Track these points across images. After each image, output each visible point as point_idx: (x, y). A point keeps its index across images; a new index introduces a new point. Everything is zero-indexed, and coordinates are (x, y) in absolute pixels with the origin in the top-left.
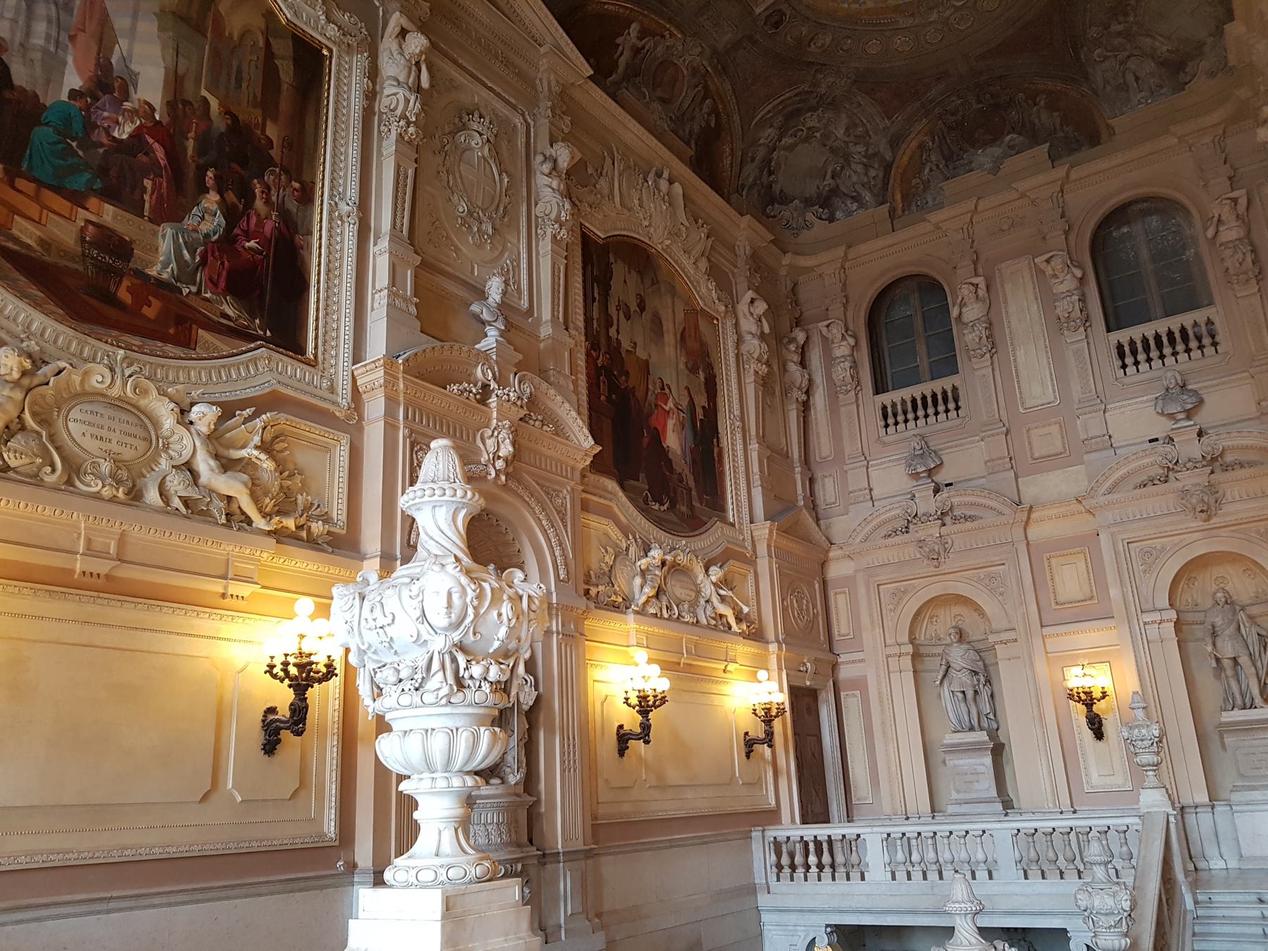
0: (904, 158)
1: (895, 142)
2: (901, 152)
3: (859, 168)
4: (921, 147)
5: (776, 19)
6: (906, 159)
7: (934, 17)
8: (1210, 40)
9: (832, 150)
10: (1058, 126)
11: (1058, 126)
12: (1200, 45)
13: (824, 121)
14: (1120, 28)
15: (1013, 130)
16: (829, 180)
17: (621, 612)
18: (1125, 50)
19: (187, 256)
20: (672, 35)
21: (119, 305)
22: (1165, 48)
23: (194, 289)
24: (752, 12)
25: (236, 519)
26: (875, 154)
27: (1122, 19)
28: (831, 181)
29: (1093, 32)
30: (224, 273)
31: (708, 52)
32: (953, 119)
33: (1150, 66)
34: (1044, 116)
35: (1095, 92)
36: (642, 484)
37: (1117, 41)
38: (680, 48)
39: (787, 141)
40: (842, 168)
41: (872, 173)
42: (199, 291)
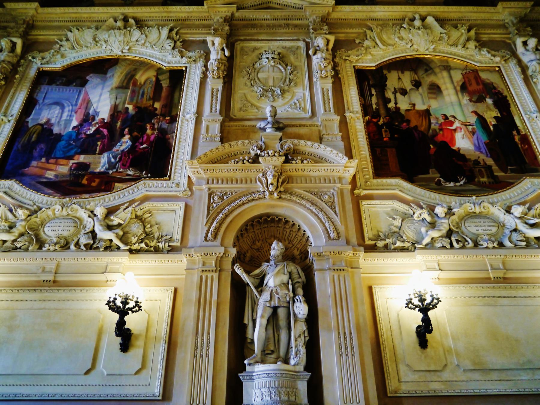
17: (411, 251)
19: (113, 160)
21: (84, 185)
23: (114, 170)
25: (109, 248)
30: (129, 160)
36: (434, 174)
42: (117, 170)
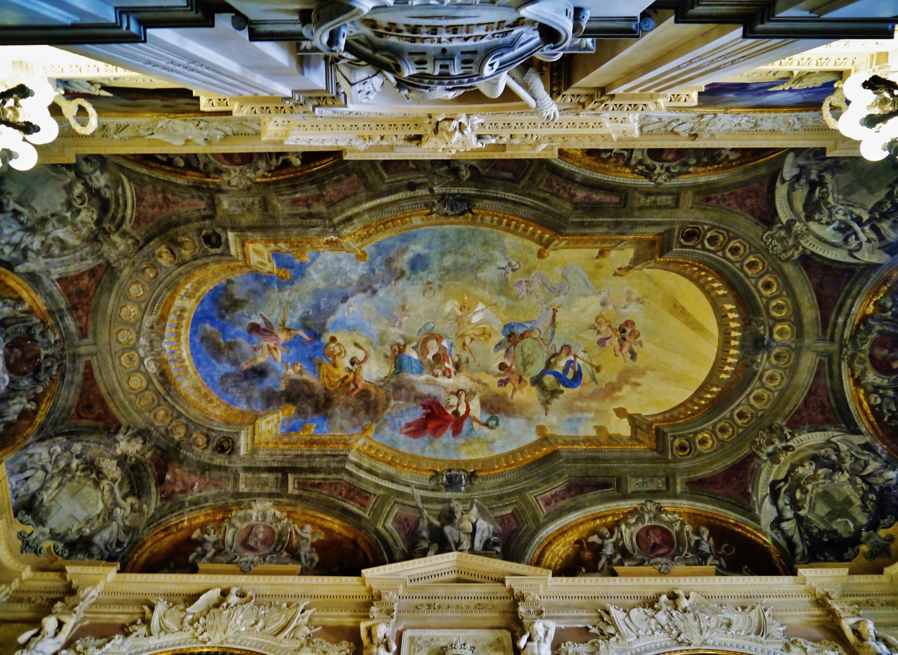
0: (12, 281)
1: (33, 278)
2: (20, 281)
3: (16, 239)
4: (20, 300)
5: (214, 241)
6: (12, 283)
7: (143, 341)
8: (46, 530)
9: (43, 221)
10: (5, 419)
11: (5, 419)
12: (41, 522)
13: (80, 226)
14: (74, 465)
15: (12, 381)
16: (13, 205)
18: (53, 468)
20: (264, 176)
22: (45, 497)
24: (233, 229)
26: (25, 258)
27: (81, 467)
28: (11, 208)
29: (77, 447)
31: (225, 187)
32: (38, 331)
33: (34, 485)
34: (18, 408)
35: (26, 447)
37: (62, 464)
38: (248, 175)
39: (79, 189)
40: (21, 223)
41: (7, 250)
